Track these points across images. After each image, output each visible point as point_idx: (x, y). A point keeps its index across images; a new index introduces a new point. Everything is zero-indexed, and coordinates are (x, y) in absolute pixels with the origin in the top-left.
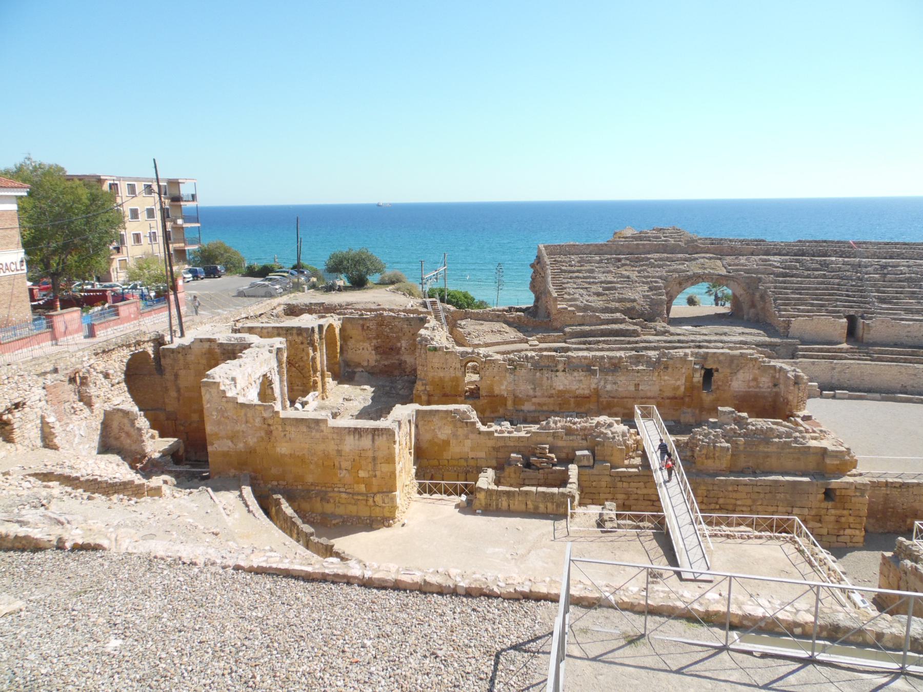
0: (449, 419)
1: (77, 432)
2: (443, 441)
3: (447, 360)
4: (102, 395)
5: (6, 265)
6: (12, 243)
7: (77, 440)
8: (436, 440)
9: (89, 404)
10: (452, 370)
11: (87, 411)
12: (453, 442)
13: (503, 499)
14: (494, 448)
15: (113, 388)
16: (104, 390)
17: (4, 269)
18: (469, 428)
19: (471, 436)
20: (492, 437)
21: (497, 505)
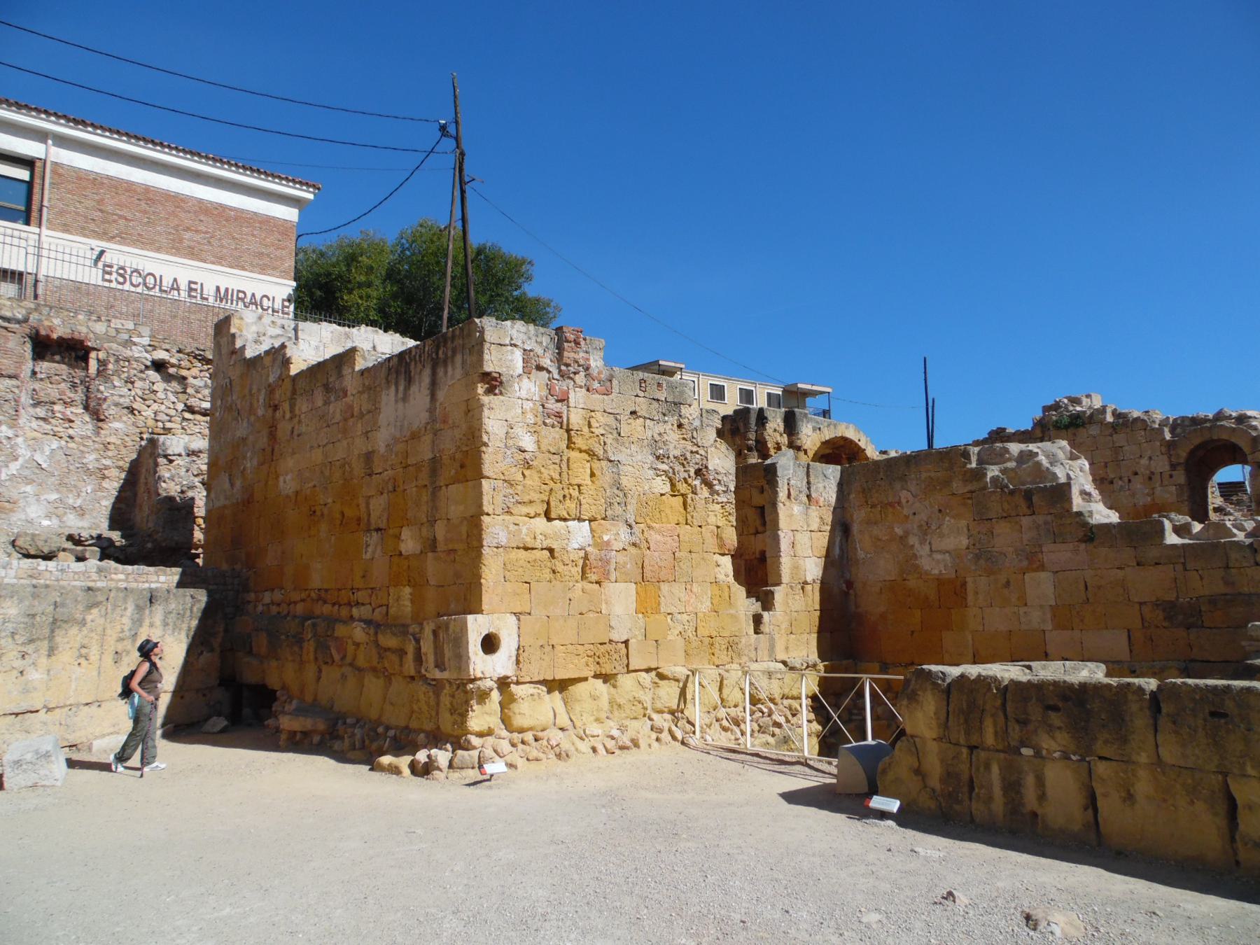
0: (958, 486)
1: (23, 451)
2: (940, 581)
3: (1117, 449)
4: (149, 413)
5: (253, 295)
6: (274, 268)
7: (14, 467)
8: (913, 583)
9: (98, 417)
10: (1138, 484)
11: (83, 426)
12: (979, 585)
13: (1046, 743)
14: (1170, 610)
15: (187, 415)
16: (155, 407)
17: (248, 300)
18: (1040, 519)
19: (1058, 554)
20: (1153, 553)
21: (1012, 787)
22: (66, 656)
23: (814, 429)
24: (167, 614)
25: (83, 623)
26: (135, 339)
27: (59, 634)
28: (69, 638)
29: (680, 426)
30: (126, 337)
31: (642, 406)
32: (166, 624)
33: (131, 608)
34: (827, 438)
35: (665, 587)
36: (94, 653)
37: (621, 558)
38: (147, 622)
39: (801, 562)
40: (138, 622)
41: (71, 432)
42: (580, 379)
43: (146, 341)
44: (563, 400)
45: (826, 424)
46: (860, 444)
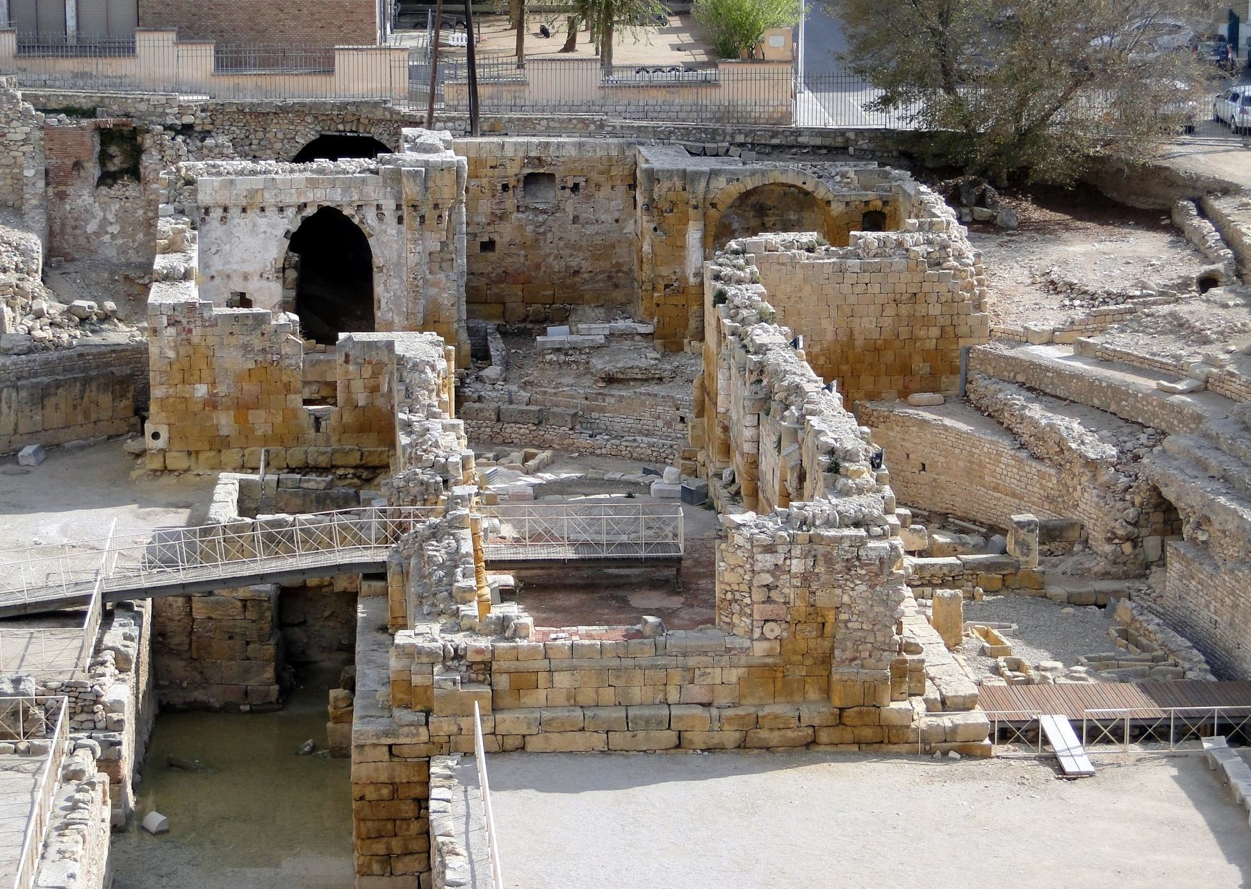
22: (49, 410)
23: (729, 181)
24: (98, 386)
25: (56, 394)
26: (168, 111)
27: (46, 402)
28: (50, 402)
29: (263, 334)
30: (161, 110)
31: (236, 329)
32: (98, 390)
33: (78, 385)
34: (750, 187)
35: (250, 411)
36: (62, 406)
37: (223, 400)
38: (88, 391)
39: (354, 396)
40: (83, 391)
41: (127, 194)
42: (199, 323)
43: (176, 110)
44: (190, 331)
45: (748, 173)
46: (804, 186)
